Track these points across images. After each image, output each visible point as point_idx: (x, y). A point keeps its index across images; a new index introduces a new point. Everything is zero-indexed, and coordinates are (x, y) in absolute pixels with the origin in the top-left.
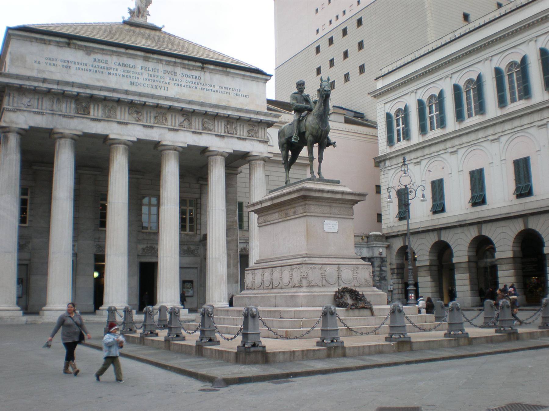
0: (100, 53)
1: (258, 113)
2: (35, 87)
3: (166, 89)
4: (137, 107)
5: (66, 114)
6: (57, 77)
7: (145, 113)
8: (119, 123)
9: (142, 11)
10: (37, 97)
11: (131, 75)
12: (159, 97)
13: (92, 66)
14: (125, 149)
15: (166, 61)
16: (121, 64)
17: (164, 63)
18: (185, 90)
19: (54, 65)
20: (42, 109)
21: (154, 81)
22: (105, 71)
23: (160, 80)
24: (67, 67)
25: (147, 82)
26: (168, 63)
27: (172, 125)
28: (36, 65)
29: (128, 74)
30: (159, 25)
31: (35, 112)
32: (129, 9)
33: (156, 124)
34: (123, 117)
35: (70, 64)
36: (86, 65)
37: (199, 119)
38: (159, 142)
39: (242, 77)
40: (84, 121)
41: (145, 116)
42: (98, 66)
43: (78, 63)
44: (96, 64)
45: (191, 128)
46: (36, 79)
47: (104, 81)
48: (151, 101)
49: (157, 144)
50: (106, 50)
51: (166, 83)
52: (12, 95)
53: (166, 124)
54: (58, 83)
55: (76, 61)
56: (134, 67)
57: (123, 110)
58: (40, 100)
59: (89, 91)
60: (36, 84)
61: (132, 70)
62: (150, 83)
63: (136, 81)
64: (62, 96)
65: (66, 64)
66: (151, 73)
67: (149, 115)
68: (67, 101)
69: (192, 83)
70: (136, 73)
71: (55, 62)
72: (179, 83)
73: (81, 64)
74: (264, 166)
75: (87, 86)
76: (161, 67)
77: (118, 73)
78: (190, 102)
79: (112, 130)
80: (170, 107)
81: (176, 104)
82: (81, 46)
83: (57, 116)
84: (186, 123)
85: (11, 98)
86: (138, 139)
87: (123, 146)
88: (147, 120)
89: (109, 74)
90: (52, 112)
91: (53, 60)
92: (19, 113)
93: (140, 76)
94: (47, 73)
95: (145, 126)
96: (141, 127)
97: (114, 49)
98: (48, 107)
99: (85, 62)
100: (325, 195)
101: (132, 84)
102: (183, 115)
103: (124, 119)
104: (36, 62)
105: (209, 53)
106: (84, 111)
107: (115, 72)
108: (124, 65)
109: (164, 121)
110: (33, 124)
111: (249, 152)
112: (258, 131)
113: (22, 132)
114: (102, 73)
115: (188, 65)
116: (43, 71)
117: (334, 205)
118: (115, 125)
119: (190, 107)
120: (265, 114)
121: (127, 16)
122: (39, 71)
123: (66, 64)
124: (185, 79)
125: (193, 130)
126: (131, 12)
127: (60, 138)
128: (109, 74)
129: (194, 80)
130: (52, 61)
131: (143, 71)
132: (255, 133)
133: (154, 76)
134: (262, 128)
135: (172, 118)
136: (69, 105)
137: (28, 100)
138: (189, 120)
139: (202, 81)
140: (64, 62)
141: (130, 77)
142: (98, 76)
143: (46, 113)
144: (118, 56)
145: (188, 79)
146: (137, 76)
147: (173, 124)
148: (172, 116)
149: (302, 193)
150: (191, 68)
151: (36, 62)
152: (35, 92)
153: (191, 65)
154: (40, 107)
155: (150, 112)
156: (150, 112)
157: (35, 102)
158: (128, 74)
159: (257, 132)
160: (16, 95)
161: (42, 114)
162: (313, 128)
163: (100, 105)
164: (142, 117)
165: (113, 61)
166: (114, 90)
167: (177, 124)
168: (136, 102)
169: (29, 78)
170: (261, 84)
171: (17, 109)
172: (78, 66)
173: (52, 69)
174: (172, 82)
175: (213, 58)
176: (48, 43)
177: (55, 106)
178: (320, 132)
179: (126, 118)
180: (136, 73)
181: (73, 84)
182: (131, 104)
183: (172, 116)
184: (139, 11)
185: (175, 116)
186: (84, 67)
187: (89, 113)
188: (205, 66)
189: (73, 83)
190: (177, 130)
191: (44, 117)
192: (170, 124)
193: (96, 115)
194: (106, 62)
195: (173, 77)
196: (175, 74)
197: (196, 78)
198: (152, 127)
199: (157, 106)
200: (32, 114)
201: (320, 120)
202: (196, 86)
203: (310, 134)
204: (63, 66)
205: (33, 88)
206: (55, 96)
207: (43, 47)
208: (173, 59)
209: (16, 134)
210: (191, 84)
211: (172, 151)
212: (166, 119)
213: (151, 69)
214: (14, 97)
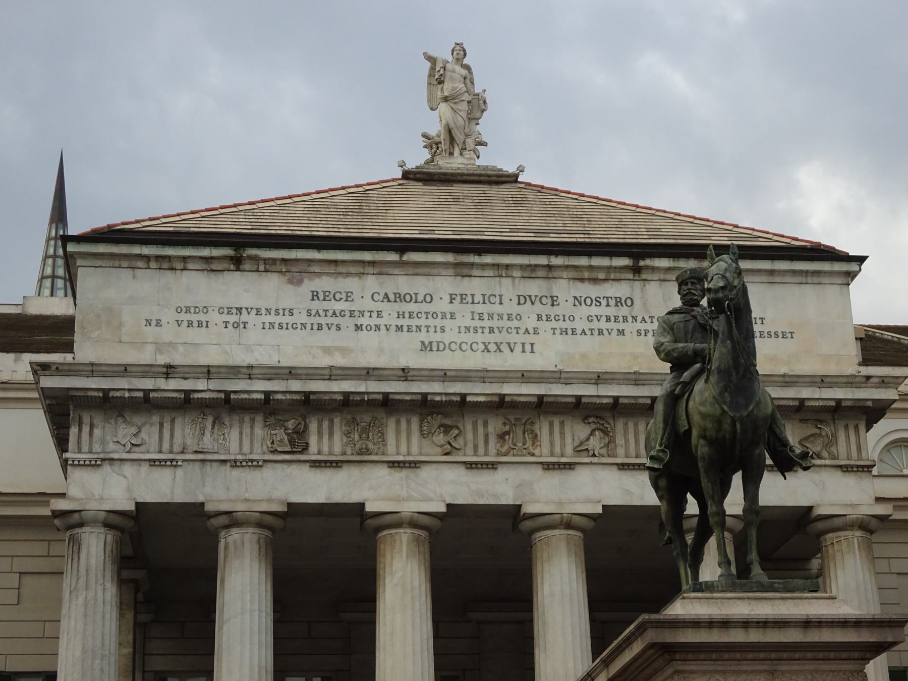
0: (327, 274)
1: (823, 381)
2: (146, 392)
3: (528, 348)
4: (441, 412)
5: (240, 457)
6: (212, 357)
7: (469, 427)
8: (393, 465)
9: (459, 137)
10: (156, 419)
11: (422, 322)
12: (504, 376)
13: (309, 313)
14: (417, 540)
15: (522, 267)
16: (392, 297)
17: (517, 273)
18: (586, 344)
19: (200, 324)
20: (171, 452)
21: (491, 330)
22: (347, 323)
23: (510, 324)
24: (236, 325)
25: (470, 337)
26: (530, 272)
27: (552, 454)
28: (151, 331)
29: (415, 322)
30: (510, 168)
31: (153, 462)
32: (425, 136)
33: (506, 455)
34: (403, 449)
35: (245, 317)
37: (636, 425)
38: (520, 506)
39: (764, 278)
40: (294, 470)
41: (470, 436)
42: (326, 311)
43: (268, 311)
44: (316, 305)
45: (615, 456)
46: (147, 371)
47: (344, 351)
48: (478, 391)
49: (514, 513)
50: (343, 262)
52: (86, 420)
53: (537, 452)
54: (208, 372)
55: (263, 305)
56: (429, 298)
57: (404, 425)
58: (167, 426)
59: (296, 386)
60: (148, 384)
61: (425, 307)
62: (479, 338)
64: (226, 407)
65: (233, 318)
66: (480, 308)
67: (481, 430)
68: (242, 422)
69: (608, 319)
70: (434, 315)
71: (202, 317)
72: (568, 325)
73: (277, 314)
74: (868, 547)
75: (291, 373)
76: (507, 288)
77: (381, 322)
78: (599, 379)
79: (371, 488)
80: (541, 397)
81: (557, 390)
82: (274, 261)
83: (215, 465)
84: (595, 443)
85: (86, 429)
86: (449, 506)
87: (409, 531)
88: (476, 447)
89: (358, 328)
90: (200, 457)
92: (107, 468)
93: (447, 323)
94: (181, 348)
95: (470, 466)
96: (461, 470)
97: (367, 256)
98: (189, 442)
99: (286, 304)
100: (737, 636)
101: (426, 347)
102: (585, 419)
103: (409, 454)
104: (149, 322)
105: (658, 223)
106: (292, 442)
107: (375, 321)
108: (400, 298)
109: (529, 443)
110: (149, 497)
111: (810, 509)
112: (835, 436)
113: (117, 520)
114: (339, 328)
115: (591, 268)
116: (172, 345)
117: (785, 667)
118: (382, 472)
119: (602, 393)
120: (850, 381)
121: (418, 158)
122: (159, 347)
123: (233, 318)
124: (585, 311)
125: (619, 460)
126: (432, 144)
127: (227, 527)
128: (358, 328)
129: (612, 311)
130: (193, 316)
131: (456, 306)
132: (827, 446)
133: (491, 316)
134: (846, 427)
135: (551, 433)
136: (247, 430)
137: (134, 430)
138: (605, 432)
139: (638, 310)
141: (419, 328)
142: (325, 338)
143: (183, 461)
145: (594, 310)
146: (438, 322)
147: (558, 449)
148: (551, 424)
149: (651, 636)
150: (601, 276)
151: (149, 322)
152: (147, 404)
153: (600, 268)
154: (166, 446)
155: (486, 424)
156: (486, 424)
157: (150, 435)
158: (415, 322)
159: (832, 441)
160: (98, 420)
161: (173, 464)
162: (704, 416)
163: (337, 421)
164: (461, 440)
165: (365, 290)
166: (369, 373)
167: (569, 450)
168: (438, 398)
169: (125, 370)
170: (832, 291)
171: (103, 460)
172: (268, 319)
173: (195, 335)
174: (544, 325)
175: (667, 235)
176: (179, 265)
177: (207, 438)
178: (727, 426)
179: (415, 449)
180: (434, 315)
181: (250, 372)
182: (425, 407)
183: (551, 424)
184: (452, 140)
185: (562, 423)
186: (287, 319)
187: (305, 449)
188: (642, 263)
189: (250, 367)
190: (570, 466)
191: (180, 472)
192: (546, 450)
193: (325, 449)
194: (348, 297)
195: (547, 310)
196: (554, 302)
197: (618, 302)
198: (492, 466)
199: (501, 405)
200: (145, 468)
201: (725, 388)
202: (621, 326)
203: (698, 439)
204: (226, 323)
205: (141, 394)
206: (207, 411)
207: (168, 277)
208: (542, 260)
209: (102, 530)
210: (603, 325)
211: (557, 532)
212: (535, 437)
213: (478, 298)
214: (92, 426)
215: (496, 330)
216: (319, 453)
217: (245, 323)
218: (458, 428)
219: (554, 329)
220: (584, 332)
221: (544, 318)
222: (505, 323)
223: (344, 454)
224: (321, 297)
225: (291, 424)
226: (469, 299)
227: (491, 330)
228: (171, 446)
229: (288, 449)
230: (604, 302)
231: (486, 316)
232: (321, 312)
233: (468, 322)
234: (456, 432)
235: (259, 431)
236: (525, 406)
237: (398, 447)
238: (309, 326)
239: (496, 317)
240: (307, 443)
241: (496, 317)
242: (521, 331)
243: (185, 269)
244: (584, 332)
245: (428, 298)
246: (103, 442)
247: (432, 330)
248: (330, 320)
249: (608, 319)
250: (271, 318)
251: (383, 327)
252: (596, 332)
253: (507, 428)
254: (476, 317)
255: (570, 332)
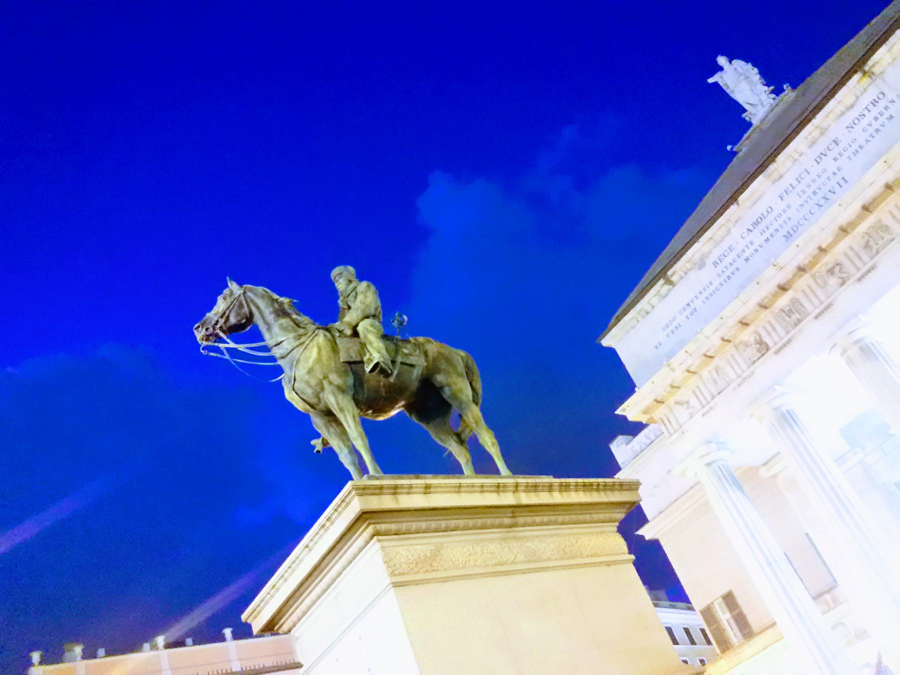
3: (842, 182)
11: (776, 225)
13: (719, 275)
16: (751, 228)
19: (677, 328)
20: (708, 403)
24: (692, 314)
34: (816, 303)
35: (693, 306)
36: (711, 283)
44: (721, 267)
51: (834, 173)
63: (787, 228)
65: (689, 310)
71: (675, 324)
72: (855, 146)
77: (756, 246)
85: (666, 422)
89: (747, 260)
91: (671, 322)
95: (859, 280)
103: (822, 303)
106: (759, 351)
108: (756, 224)
114: (738, 269)
123: (689, 310)
124: (858, 128)
128: (747, 260)
129: (875, 112)
133: (809, 186)
137: (685, 406)
139: (891, 95)
140: (684, 310)
141: (777, 230)
144: (737, 221)
145: (864, 122)
146: (784, 217)
158: (771, 230)
174: (843, 161)
179: (822, 298)
180: (780, 215)
186: (712, 288)
188: (866, 68)
196: (836, 142)
197: (874, 103)
206: (710, 368)
210: (876, 125)
212: (886, 229)
213: (795, 183)
215: (817, 191)
216: (776, 344)
217: (695, 309)
218: (838, 264)
219: (849, 157)
220: (867, 141)
221: (838, 157)
222: (819, 182)
223: (788, 333)
224: (718, 261)
225: (752, 340)
226: (791, 188)
227: (815, 193)
228: (705, 399)
229: (760, 355)
230: (866, 112)
231: (806, 189)
232: (725, 270)
233: (800, 201)
234: (838, 268)
235: (739, 359)
236: (859, 219)
237: (812, 303)
238: (724, 283)
239: (811, 183)
240: (767, 345)
241: (811, 183)
242: (831, 178)
243: (653, 307)
244: (867, 141)
245: (769, 210)
246: (678, 423)
247: (784, 225)
248: (731, 269)
249: (876, 119)
250: (706, 294)
251: (759, 248)
252: (875, 134)
253: (867, 238)
254: (801, 194)
255: (859, 149)
